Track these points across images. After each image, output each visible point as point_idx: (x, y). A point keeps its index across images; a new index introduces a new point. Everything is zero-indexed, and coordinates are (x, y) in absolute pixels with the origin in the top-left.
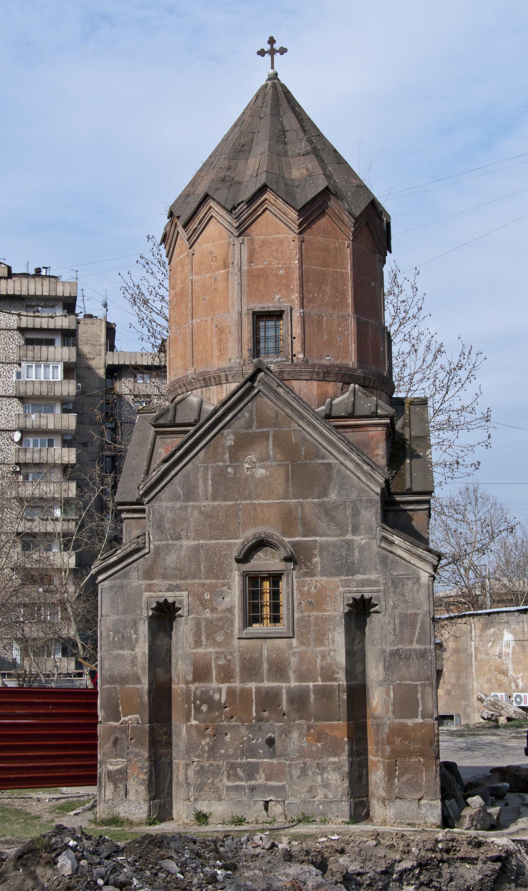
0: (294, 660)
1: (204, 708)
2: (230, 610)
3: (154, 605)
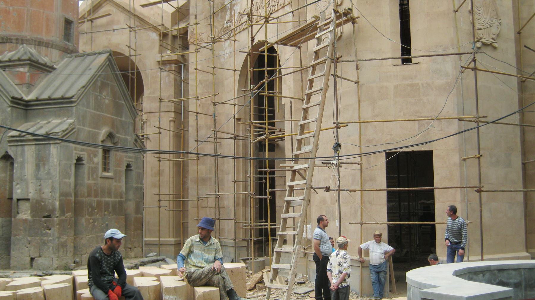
0: (113, 188)
1: (90, 210)
2: (98, 164)
3: (77, 158)
